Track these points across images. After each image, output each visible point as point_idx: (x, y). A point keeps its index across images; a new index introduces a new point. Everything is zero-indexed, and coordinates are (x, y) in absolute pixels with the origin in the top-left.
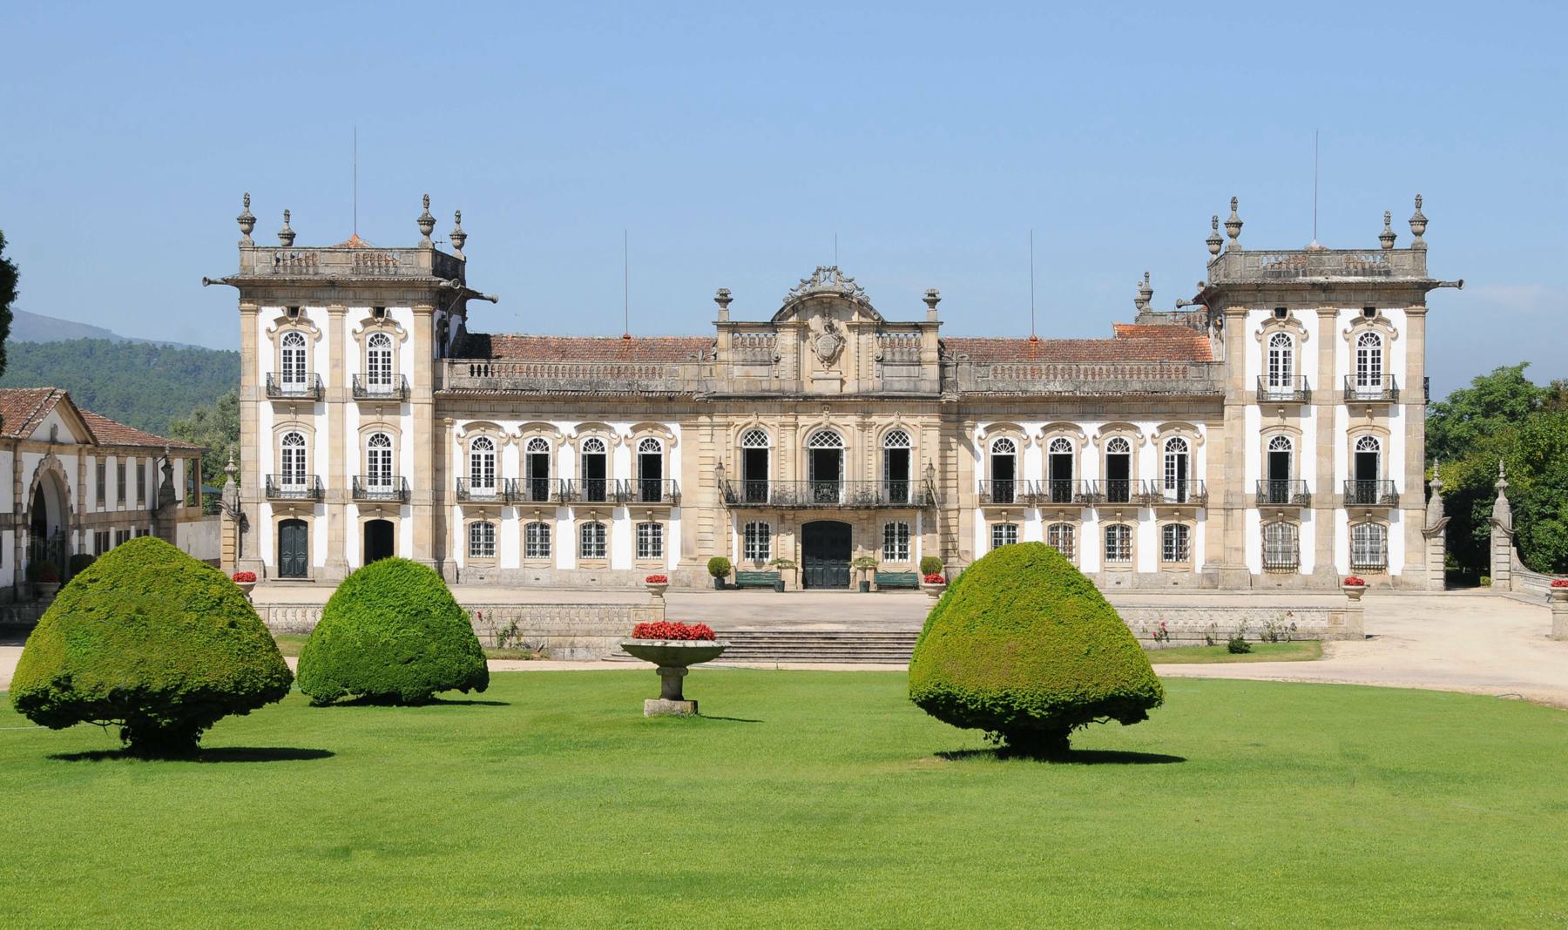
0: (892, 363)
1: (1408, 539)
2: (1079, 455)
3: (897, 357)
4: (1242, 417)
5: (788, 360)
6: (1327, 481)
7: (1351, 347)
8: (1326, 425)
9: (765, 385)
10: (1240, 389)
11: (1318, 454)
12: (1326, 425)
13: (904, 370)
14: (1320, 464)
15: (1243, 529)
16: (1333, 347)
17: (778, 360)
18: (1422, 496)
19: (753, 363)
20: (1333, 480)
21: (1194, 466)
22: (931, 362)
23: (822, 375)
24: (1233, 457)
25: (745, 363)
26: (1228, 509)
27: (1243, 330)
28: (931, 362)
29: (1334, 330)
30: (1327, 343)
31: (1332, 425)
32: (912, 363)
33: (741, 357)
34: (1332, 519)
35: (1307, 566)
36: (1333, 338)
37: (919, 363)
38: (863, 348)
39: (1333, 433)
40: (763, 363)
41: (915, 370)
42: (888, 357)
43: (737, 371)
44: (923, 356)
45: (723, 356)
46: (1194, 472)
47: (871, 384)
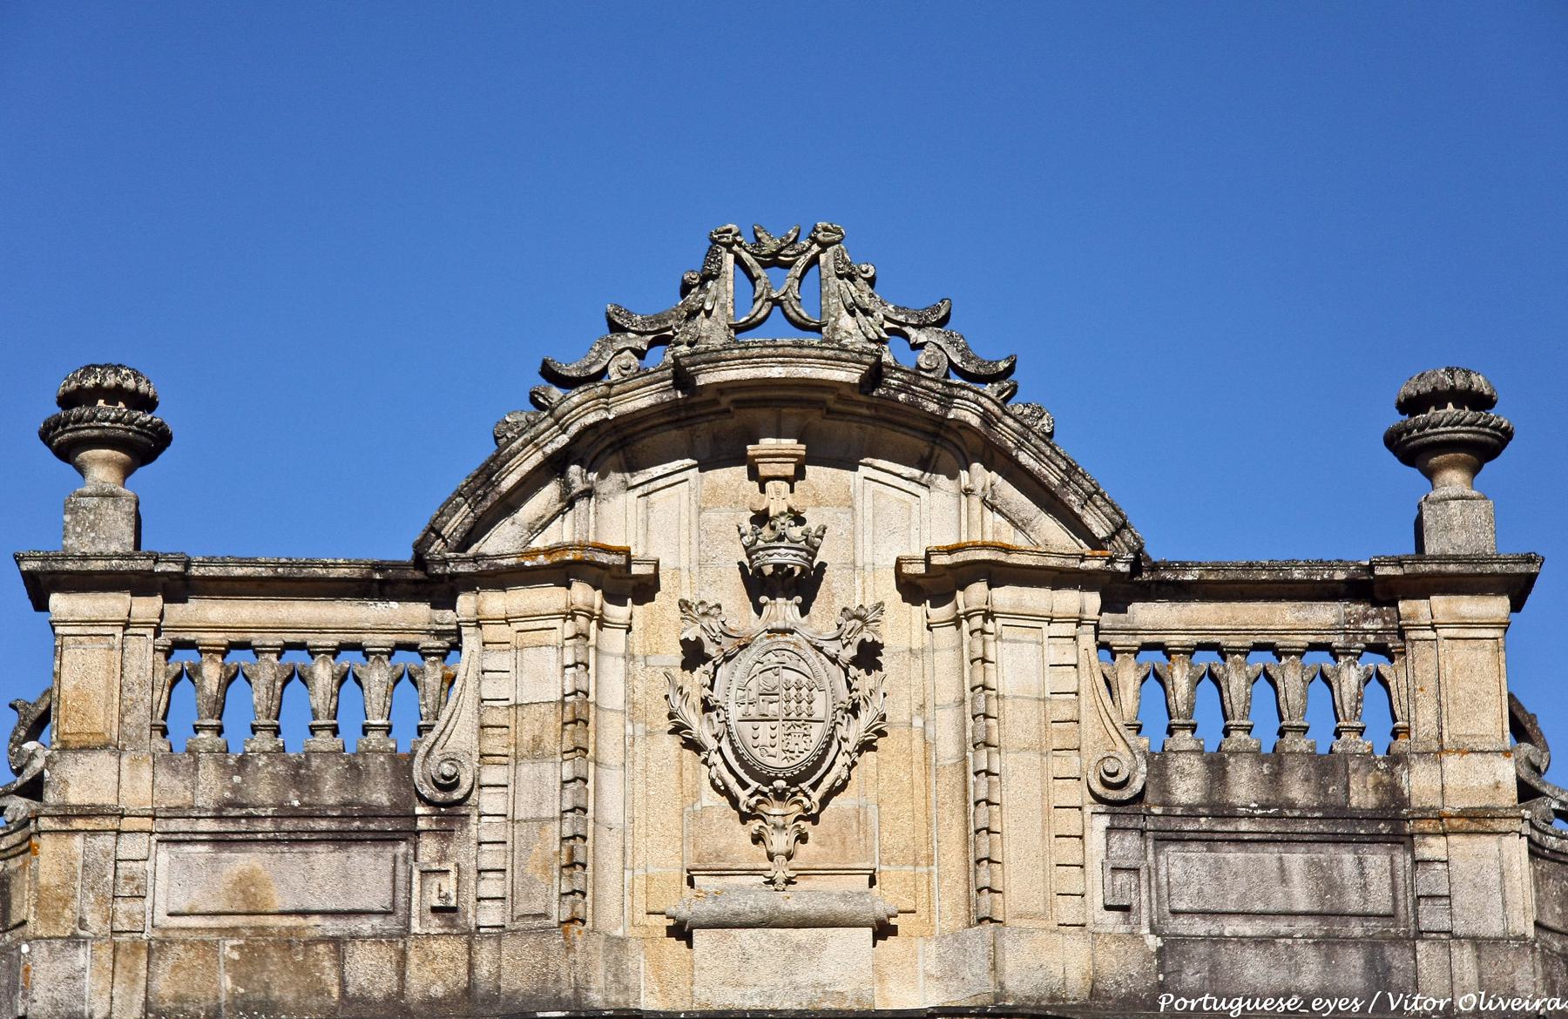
0: (1214, 824)
3: (1244, 787)
5: (514, 800)
9: (368, 969)
13: (1294, 876)
17: (452, 810)
19: (296, 829)
22: (1478, 820)
23: (749, 895)
25: (232, 828)
28: (1478, 820)
32: (1341, 827)
33: (210, 786)
37: (1394, 824)
38: (1016, 724)
40: (356, 829)
41: (1369, 876)
42: (1187, 788)
43: (178, 885)
44: (1419, 783)
45: (83, 781)
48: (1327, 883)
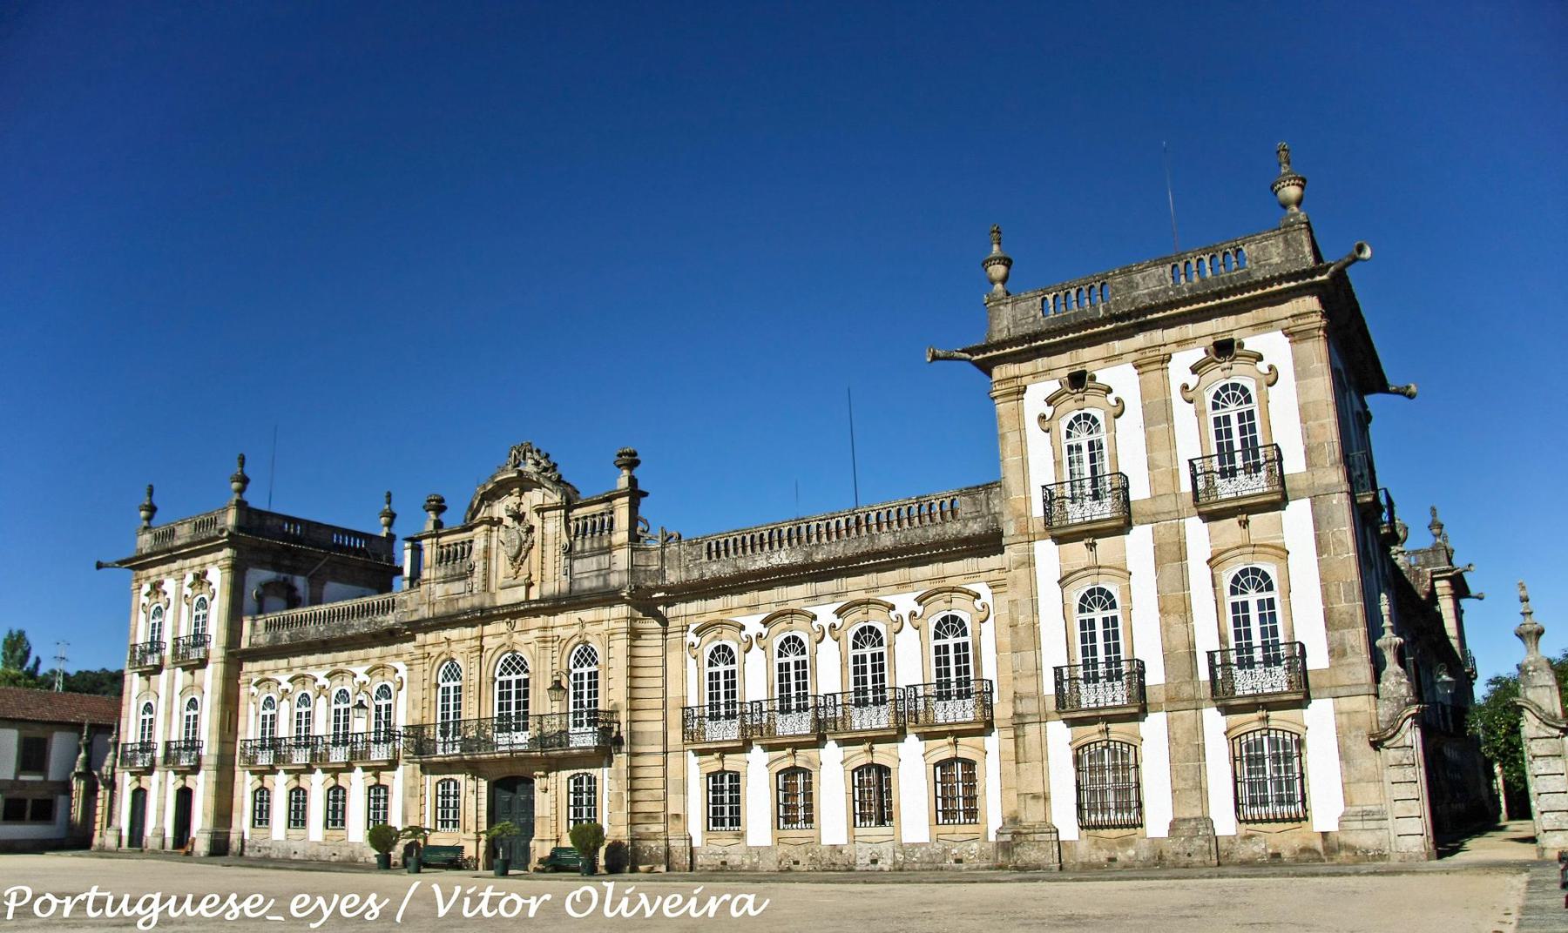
1: (1344, 755)
2: (814, 659)
4: (1029, 563)
6: (1181, 656)
7: (1199, 413)
8: (1171, 555)
10: (1023, 516)
11: (1162, 611)
12: (1171, 555)
14: (1165, 629)
15: (1044, 758)
16: (1169, 419)
18: (1364, 673)
20: (1193, 655)
21: (977, 658)
22: (621, 546)
24: (1024, 636)
26: (1019, 722)
27: (1020, 416)
28: (621, 546)
29: (1166, 389)
30: (1158, 416)
31: (1181, 555)
34: (1198, 729)
35: (1157, 819)
36: (1168, 404)
39: (1184, 570)
41: (604, 560)
46: (978, 669)
47: (552, 583)
48: (599, 563)
